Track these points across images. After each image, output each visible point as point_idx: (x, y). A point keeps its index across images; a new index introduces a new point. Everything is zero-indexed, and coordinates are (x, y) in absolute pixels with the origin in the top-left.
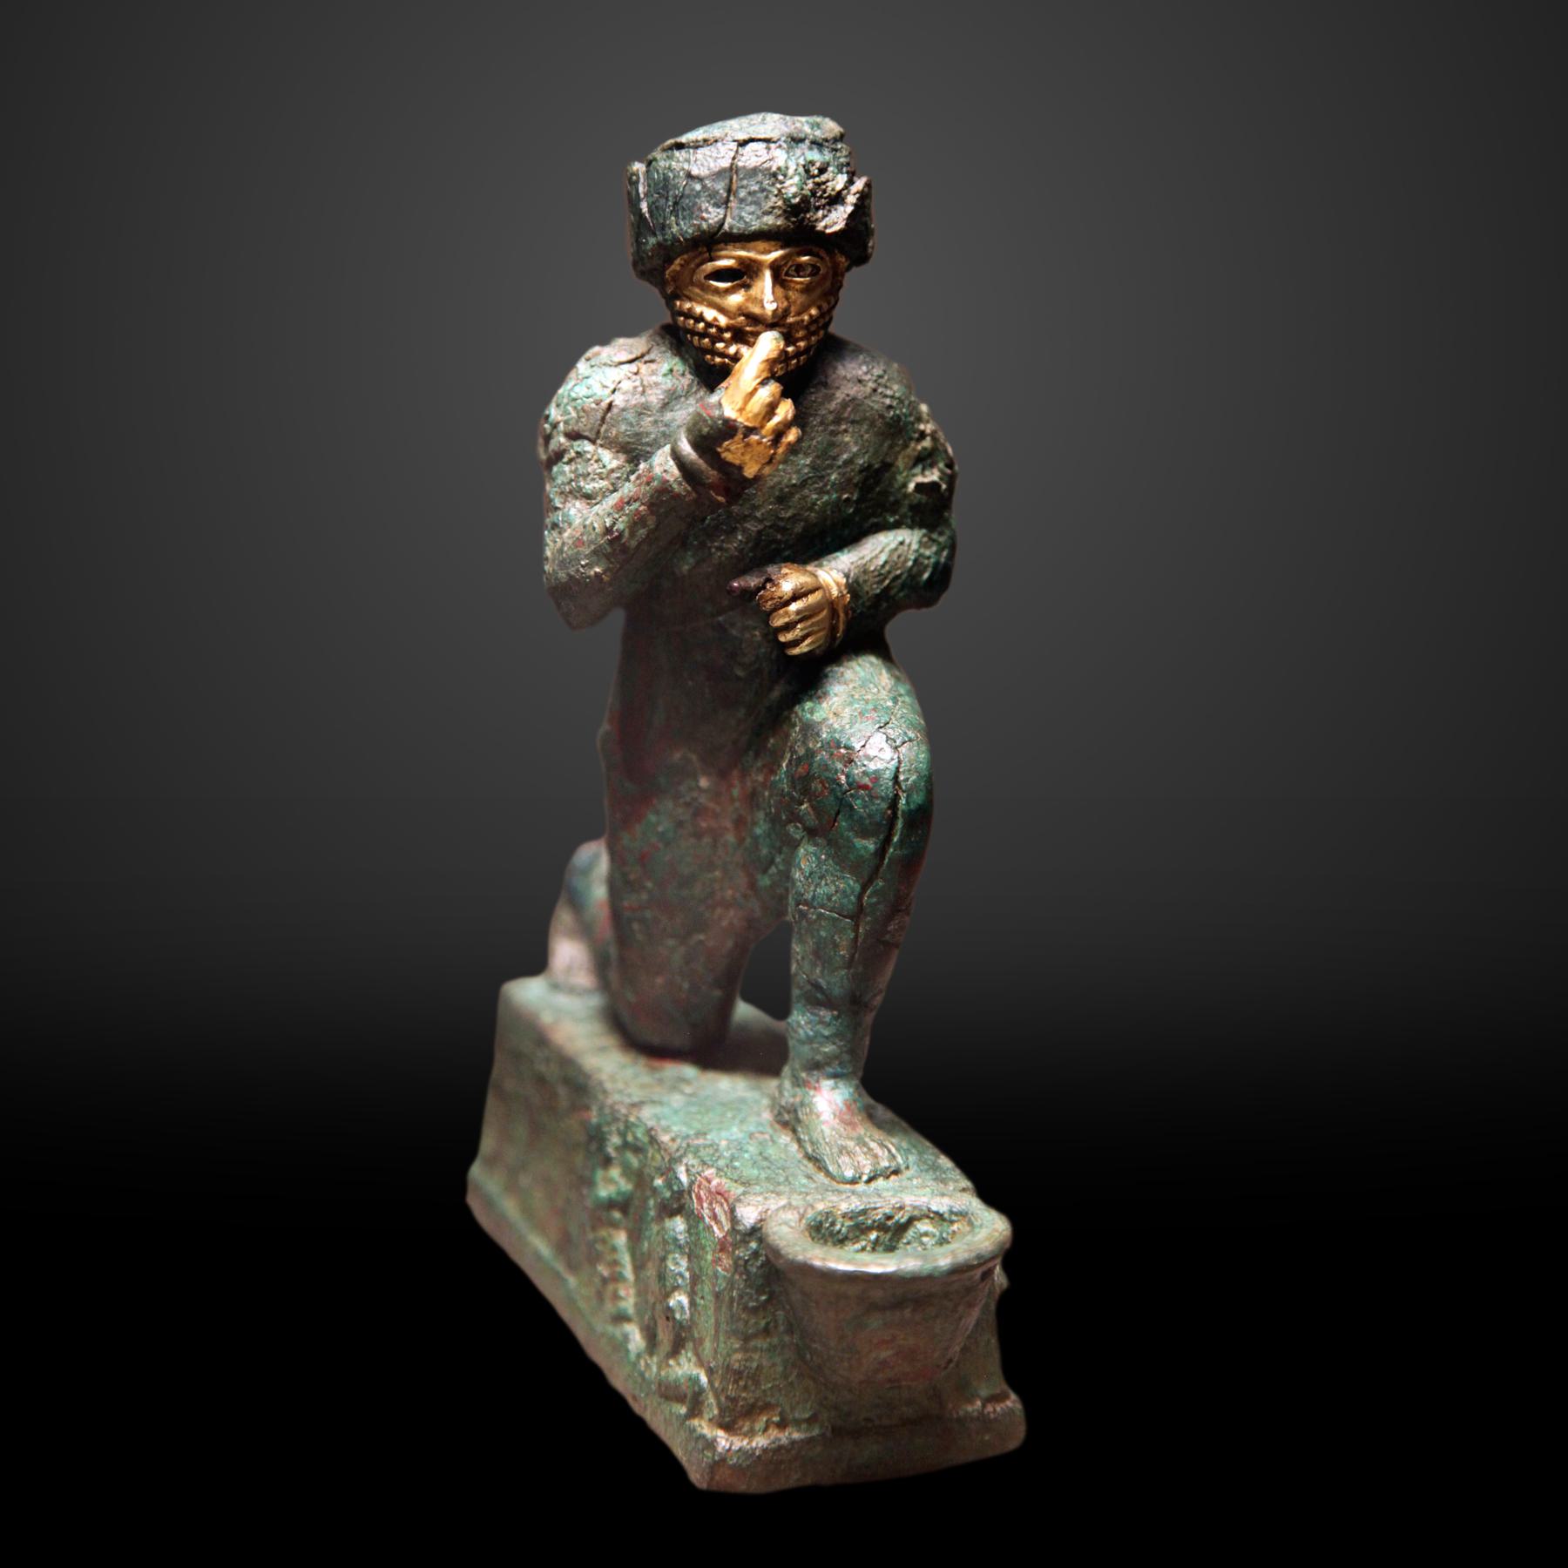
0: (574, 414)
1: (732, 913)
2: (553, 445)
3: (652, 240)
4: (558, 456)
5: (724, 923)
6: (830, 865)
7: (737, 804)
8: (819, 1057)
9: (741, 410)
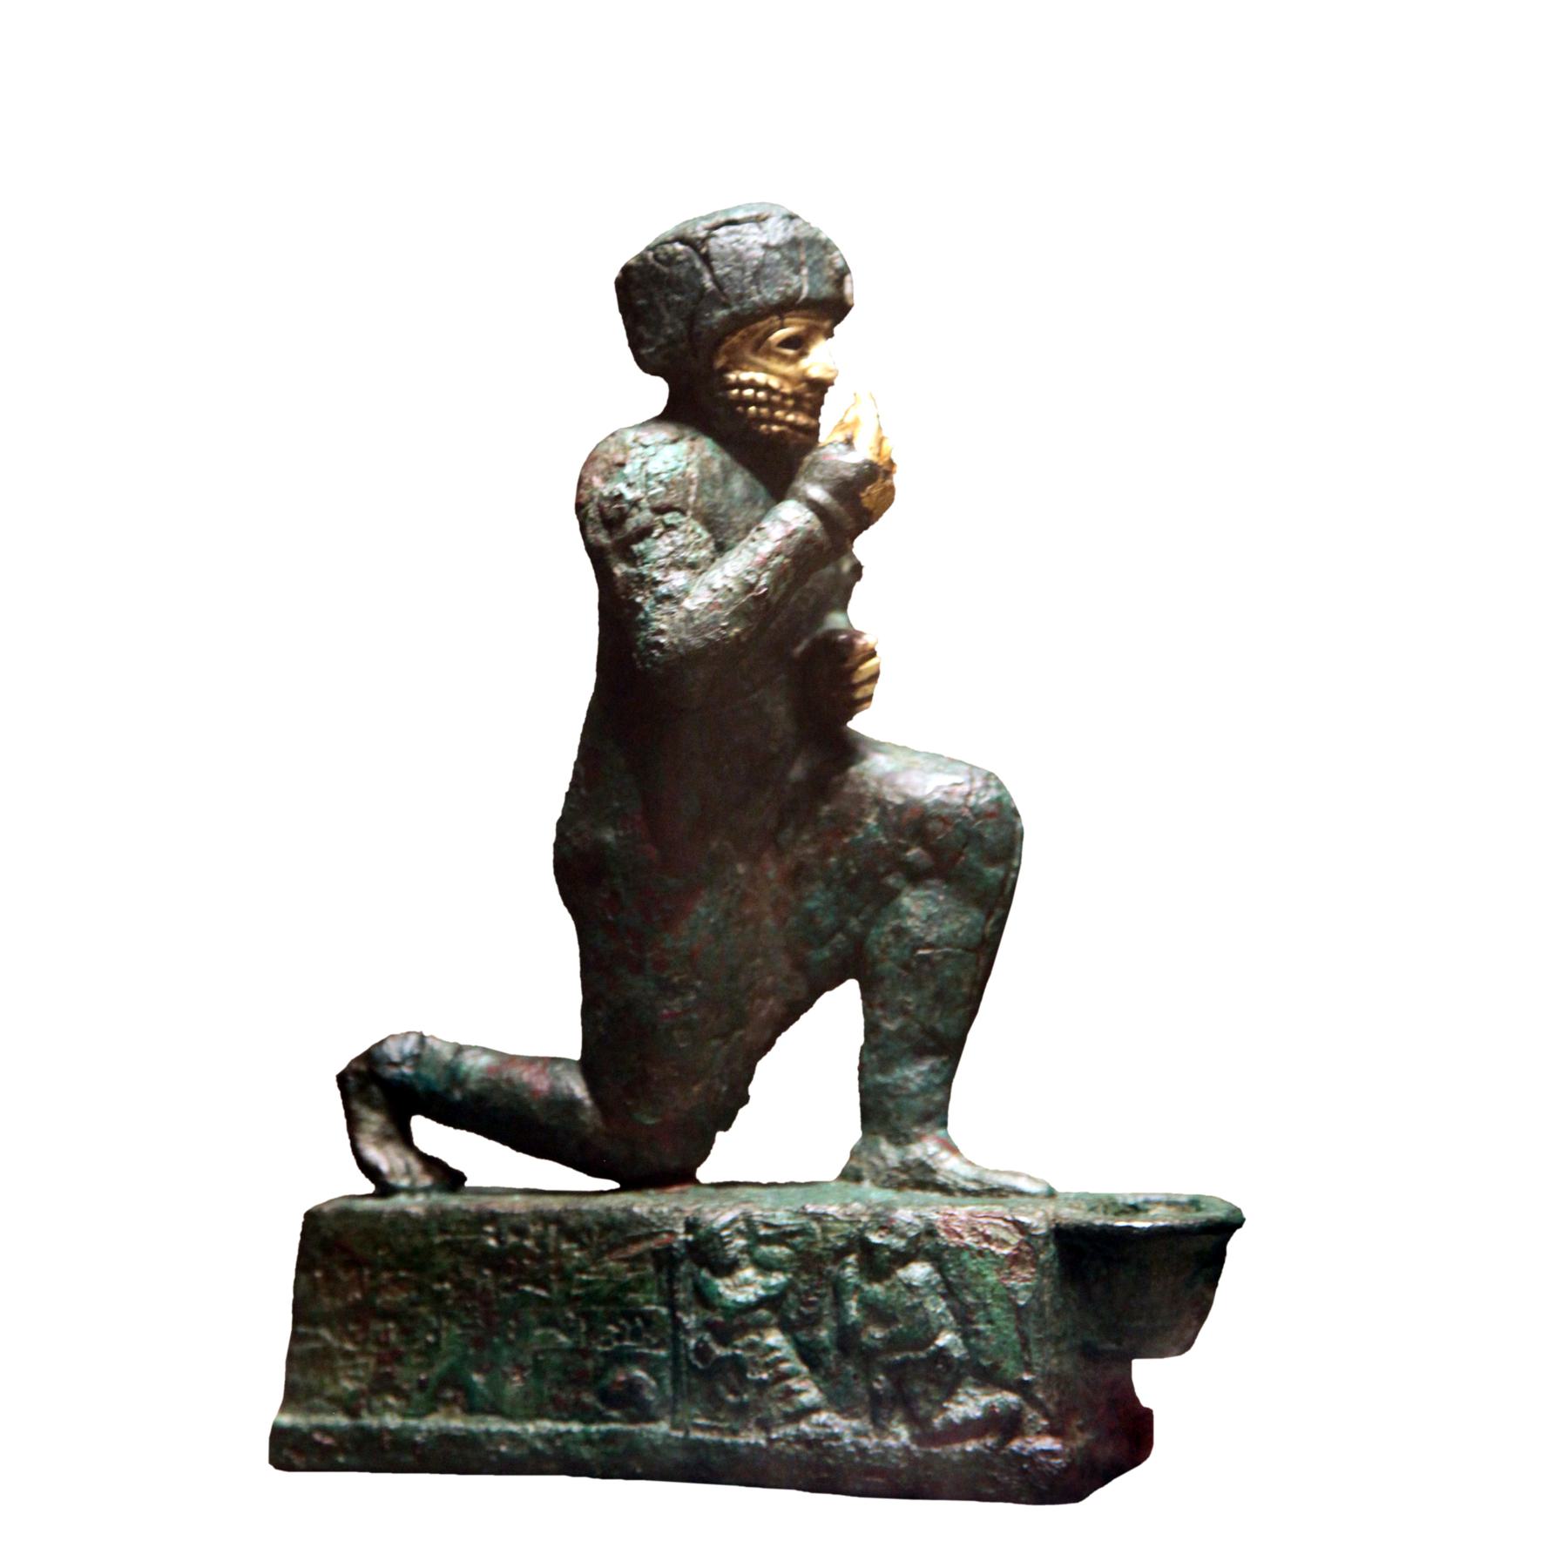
0: (661, 489)
1: (771, 1002)
2: (631, 524)
3: (721, 313)
4: (644, 533)
5: (763, 1013)
6: (952, 905)
7: (774, 886)
8: (932, 1108)
9: (879, 455)
